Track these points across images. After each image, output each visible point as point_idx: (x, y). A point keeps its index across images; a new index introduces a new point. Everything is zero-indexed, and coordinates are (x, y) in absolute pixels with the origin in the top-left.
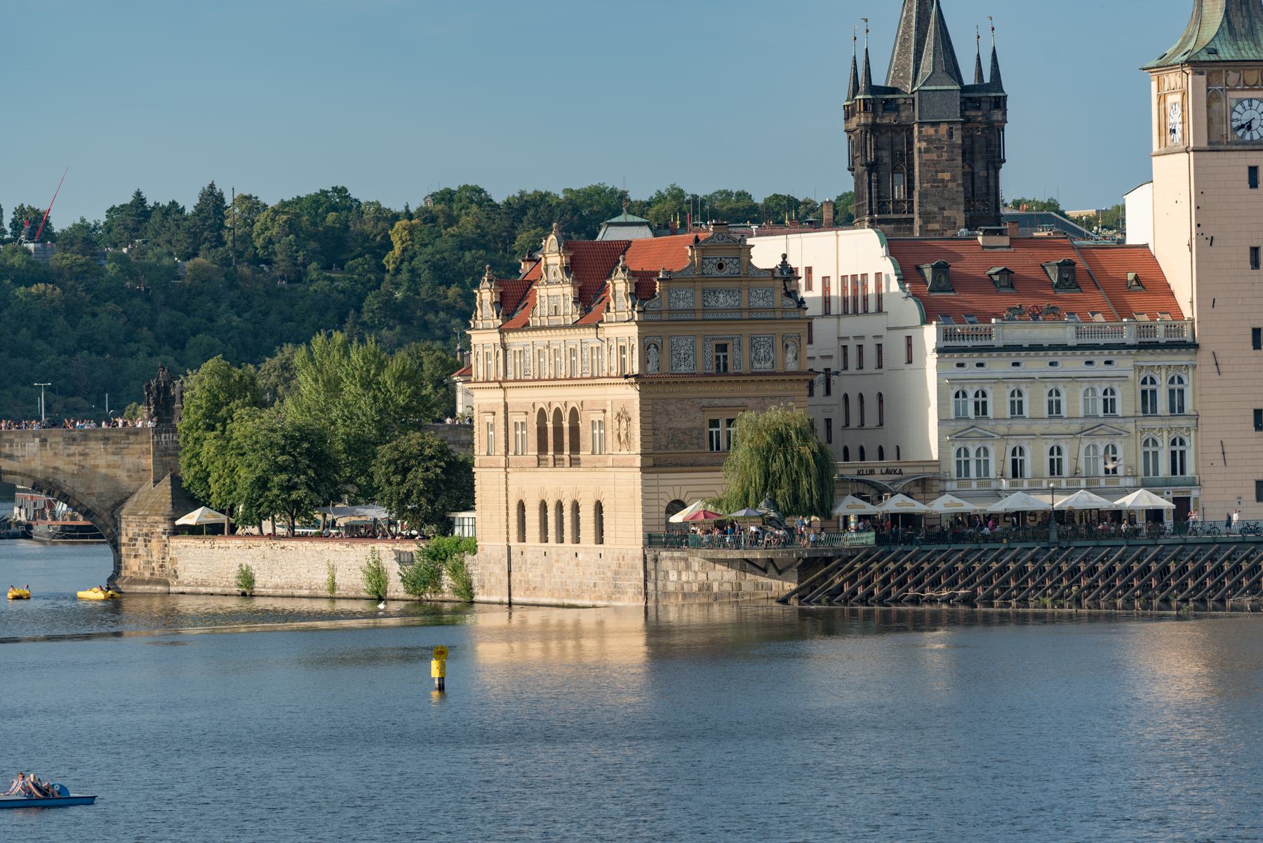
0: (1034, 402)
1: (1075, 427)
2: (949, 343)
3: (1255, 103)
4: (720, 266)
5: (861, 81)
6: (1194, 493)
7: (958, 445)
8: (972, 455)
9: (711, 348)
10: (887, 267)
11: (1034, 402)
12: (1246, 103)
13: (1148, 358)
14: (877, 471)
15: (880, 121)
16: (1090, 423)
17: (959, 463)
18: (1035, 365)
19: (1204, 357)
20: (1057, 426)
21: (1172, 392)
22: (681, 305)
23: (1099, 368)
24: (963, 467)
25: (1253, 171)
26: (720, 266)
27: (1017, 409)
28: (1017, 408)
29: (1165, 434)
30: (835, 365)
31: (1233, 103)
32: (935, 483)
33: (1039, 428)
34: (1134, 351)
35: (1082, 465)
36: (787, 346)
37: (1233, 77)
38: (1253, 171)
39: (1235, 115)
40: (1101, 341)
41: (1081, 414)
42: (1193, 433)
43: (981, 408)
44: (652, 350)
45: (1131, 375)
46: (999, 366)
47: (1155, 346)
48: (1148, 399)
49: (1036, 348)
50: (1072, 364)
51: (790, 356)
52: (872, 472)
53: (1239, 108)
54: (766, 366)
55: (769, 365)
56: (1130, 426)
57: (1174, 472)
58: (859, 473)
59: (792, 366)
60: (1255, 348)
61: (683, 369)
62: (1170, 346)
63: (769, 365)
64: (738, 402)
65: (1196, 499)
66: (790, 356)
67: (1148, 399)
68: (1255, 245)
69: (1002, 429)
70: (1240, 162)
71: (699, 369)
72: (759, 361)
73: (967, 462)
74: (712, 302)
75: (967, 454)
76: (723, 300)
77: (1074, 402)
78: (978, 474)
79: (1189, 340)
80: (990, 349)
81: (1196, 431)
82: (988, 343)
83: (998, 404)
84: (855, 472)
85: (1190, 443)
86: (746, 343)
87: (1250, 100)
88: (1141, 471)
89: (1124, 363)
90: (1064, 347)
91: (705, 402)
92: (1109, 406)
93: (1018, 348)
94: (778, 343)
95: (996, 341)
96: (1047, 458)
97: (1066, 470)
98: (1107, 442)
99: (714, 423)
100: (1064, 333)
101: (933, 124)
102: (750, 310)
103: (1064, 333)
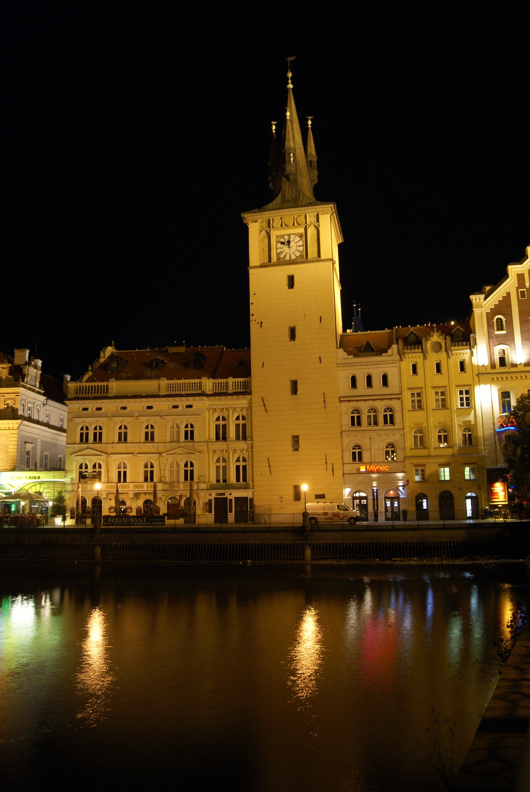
3: (292, 237)
21: (237, 426)
27: (123, 438)
28: (123, 438)
35: (167, 474)
40: (183, 393)
41: (168, 440)
56: (203, 447)
57: (238, 480)
79: (249, 391)
87: (289, 235)
92: (190, 435)
96: (142, 470)
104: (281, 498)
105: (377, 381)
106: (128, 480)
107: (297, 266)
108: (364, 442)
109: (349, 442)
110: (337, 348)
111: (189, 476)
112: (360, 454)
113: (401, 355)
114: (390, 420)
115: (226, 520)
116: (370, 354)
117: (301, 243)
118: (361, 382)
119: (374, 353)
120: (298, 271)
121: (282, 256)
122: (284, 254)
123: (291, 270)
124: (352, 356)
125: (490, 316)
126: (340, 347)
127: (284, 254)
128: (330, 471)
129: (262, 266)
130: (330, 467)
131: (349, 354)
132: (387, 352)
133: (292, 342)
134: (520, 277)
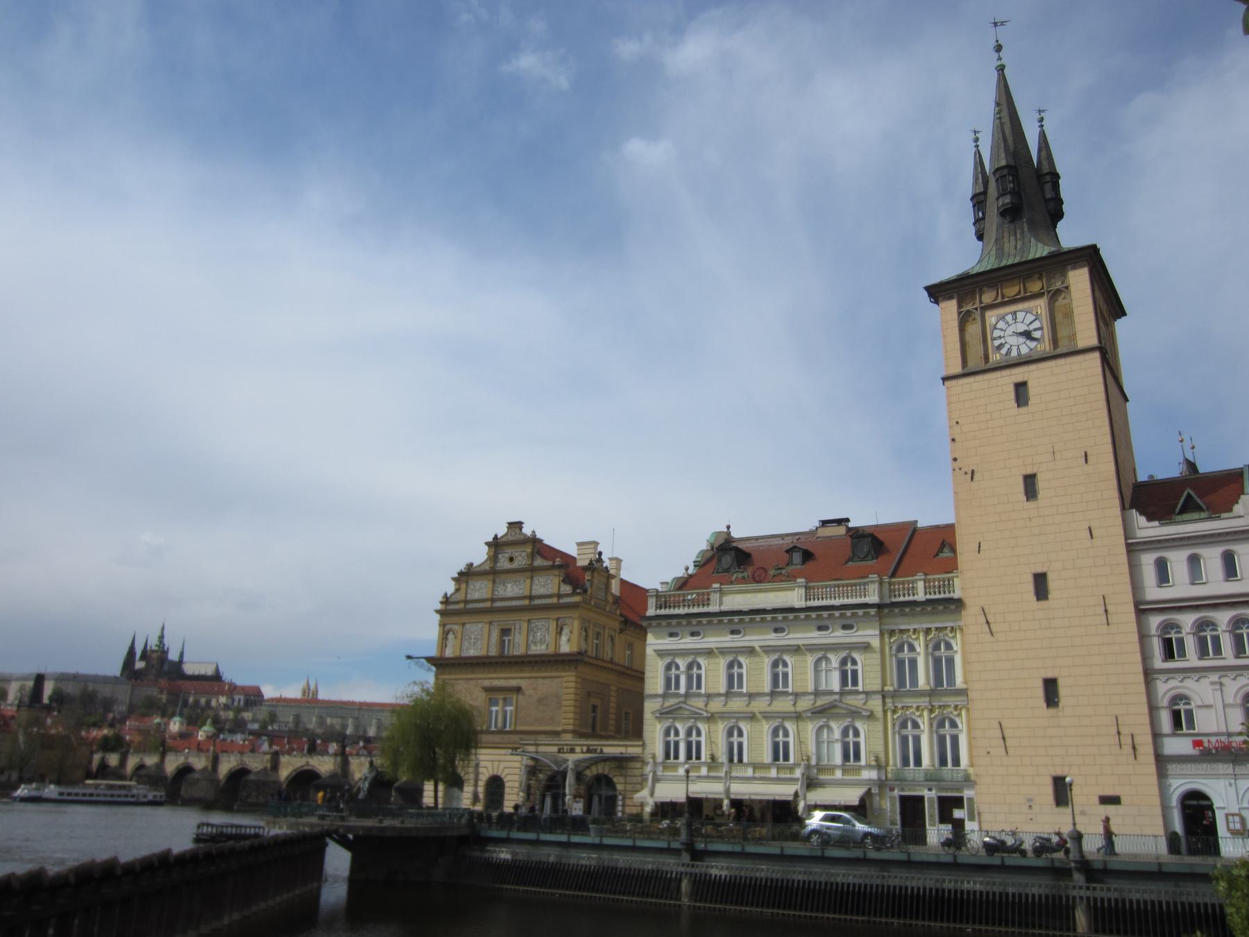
0: (757, 674)
1: (805, 704)
2: (663, 612)
3: (1020, 316)
4: (511, 559)
6: (967, 793)
7: (667, 723)
8: (682, 735)
9: (495, 634)
12: (1009, 318)
14: (578, 749)
16: (821, 702)
17: (667, 744)
19: (970, 616)
22: (477, 596)
23: (837, 635)
24: (670, 751)
25: (1021, 391)
26: (511, 559)
29: (926, 713)
31: (993, 320)
32: (638, 765)
34: (873, 611)
36: (561, 629)
38: (1021, 391)
39: (996, 333)
40: (837, 602)
41: (811, 688)
42: (964, 712)
44: (451, 636)
45: (875, 643)
47: (915, 603)
51: (564, 638)
52: (572, 751)
53: (1001, 325)
55: (543, 647)
57: (943, 762)
58: (559, 751)
59: (565, 648)
60: (1038, 599)
61: (472, 653)
62: (929, 602)
63: (543, 647)
64: (514, 683)
65: (970, 800)
68: (1029, 471)
71: (482, 653)
72: (536, 644)
73: (677, 744)
75: (677, 733)
78: (689, 757)
81: (968, 710)
82: (705, 609)
83: (714, 675)
84: (555, 749)
85: (962, 724)
86: (525, 625)
87: (1015, 313)
90: (792, 610)
91: (487, 683)
94: (553, 625)
95: (713, 608)
98: (846, 722)
102: (531, 598)
103: (793, 597)
104: (1030, 800)
106: (745, 760)
107: (1033, 367)
108: (1200, 691)
110: (1123, 508)
112: (1190, 714)
115: (921, 839)
116: (1196, 515)
117: (1037, 324)
119: (1203, 515)
121: (1004, 351)
122: (1007, 347)
123: (1019, 374)
124: (1156, 523)
126: (1132, 507)
127: (1007, 347)
128: (1128, 749)
130: (1127, 740)
131: (1150, 519)
132: (1231, 510)
133: (1032, 504)
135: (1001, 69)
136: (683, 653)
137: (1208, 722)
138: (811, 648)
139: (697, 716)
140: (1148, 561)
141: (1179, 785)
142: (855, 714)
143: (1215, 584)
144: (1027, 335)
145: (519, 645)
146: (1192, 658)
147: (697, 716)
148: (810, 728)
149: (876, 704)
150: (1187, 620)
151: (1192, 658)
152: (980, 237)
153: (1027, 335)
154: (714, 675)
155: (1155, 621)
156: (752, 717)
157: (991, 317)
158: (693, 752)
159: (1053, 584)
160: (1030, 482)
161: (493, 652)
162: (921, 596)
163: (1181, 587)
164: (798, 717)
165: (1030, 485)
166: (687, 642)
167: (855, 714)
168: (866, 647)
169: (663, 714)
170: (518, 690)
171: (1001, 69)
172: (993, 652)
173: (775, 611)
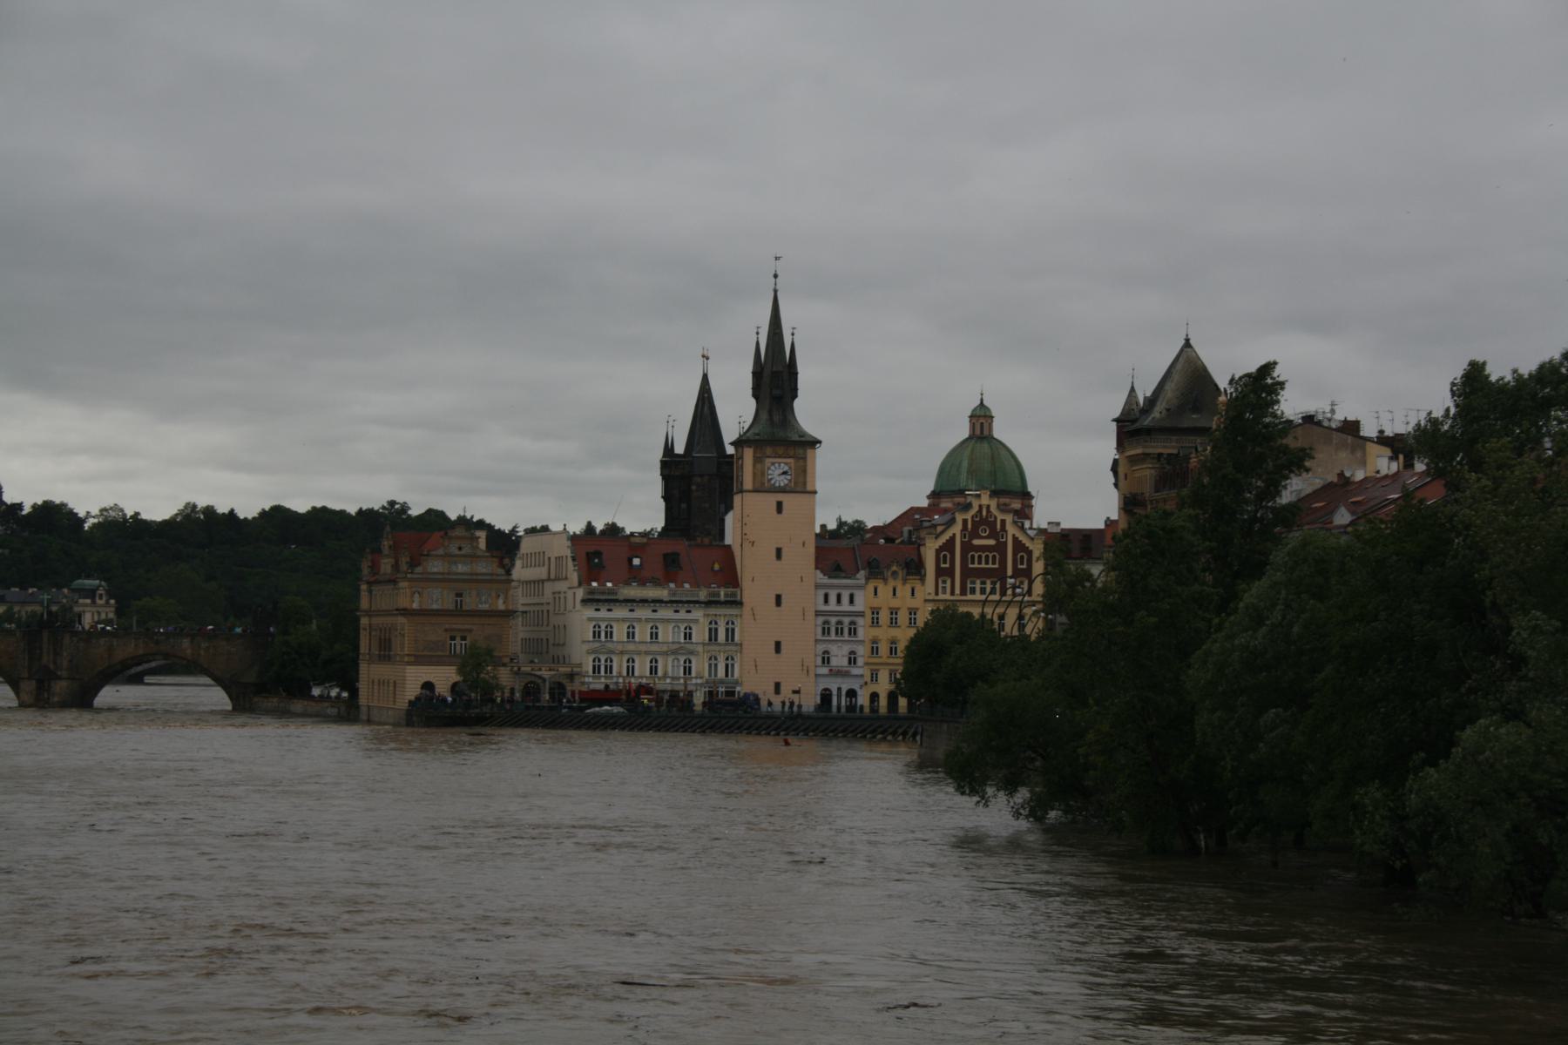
0: (643, 633)
1: (665, 648)
5: (669, 449)
10: (568, 553)
11: (643, 633)
13: (712, 611)
15: (675, 470)
18: (643, 613)
19: (746, 609)
20: (654, 648)
23: (682, 615)
24: (596, 669)
27: (631, 635)
28: (631, 635)
30: (551, 608)
33: (643, 648)
37: (769, 451)
43: (609, 635)
46: (620, 612)
48: (713, 634)
49: (644, 601)
50: (666, 613)
51: (501, 601)
54: (485, 607)
56: (700, 649)
61: (435, 607)
66: (501, 601)
67: (713, 634)
69: (620, 647)
70: (772, 499)
71: (446, 606)
74: (454, 569)
76: (461, 568)
77: (667, 634)
80: (617, 601)
83: (620, 633)
85: (737, 658)
88: (706, 674)
89: (698, 614)
90: (660, 601)
92: (688, 636)
93: (633, 601)
97: (660, 673)
99: (453, 638)
100: (663, 593)
101: (701, 476)
103: (663, 593)
105: (845, 599)
108: (833, 649)
109: (821, 648)
111: (687, 671)
113: (868, 579)
114: (853, 631)
118: (833, 599)
120: (786, 499)
123: (780, 497)
125: (938, 552)
129: (755, 491)
134: (965, 522)
135: (776, 291)
136: (603, 620)
137: (834, 662)
138: (668, 621)
139: (612, 652)
140: (821, 593)
141: (822, 687)
142: (692, 653)
143: (845, 606)
144: (785, 473)
145: (470, 602)
146: (833, 637)
147: (612, 652)
148: (670, 659)
149: (700, 649)
150: (833, 620)
151: (833, 637)
152: (755, 396)
153: (785, 473)
154: (620, 633)
155: (821, 620)
156: (639, 653)
157: (768, 461)
158: (609, 669)
159: (784, 600)
160: (779, 552)
161: (451, 607)
162: (722, 598)
163: (833, 606)
164: (666, 654)
165: (779, 552)
166: (603, 614)
167: (692, 653)
168: (696, 621)
169: (594, 652)
170: (470, 631)
171: (776, 291)
172: (756, 625)
173: (654, 601)
